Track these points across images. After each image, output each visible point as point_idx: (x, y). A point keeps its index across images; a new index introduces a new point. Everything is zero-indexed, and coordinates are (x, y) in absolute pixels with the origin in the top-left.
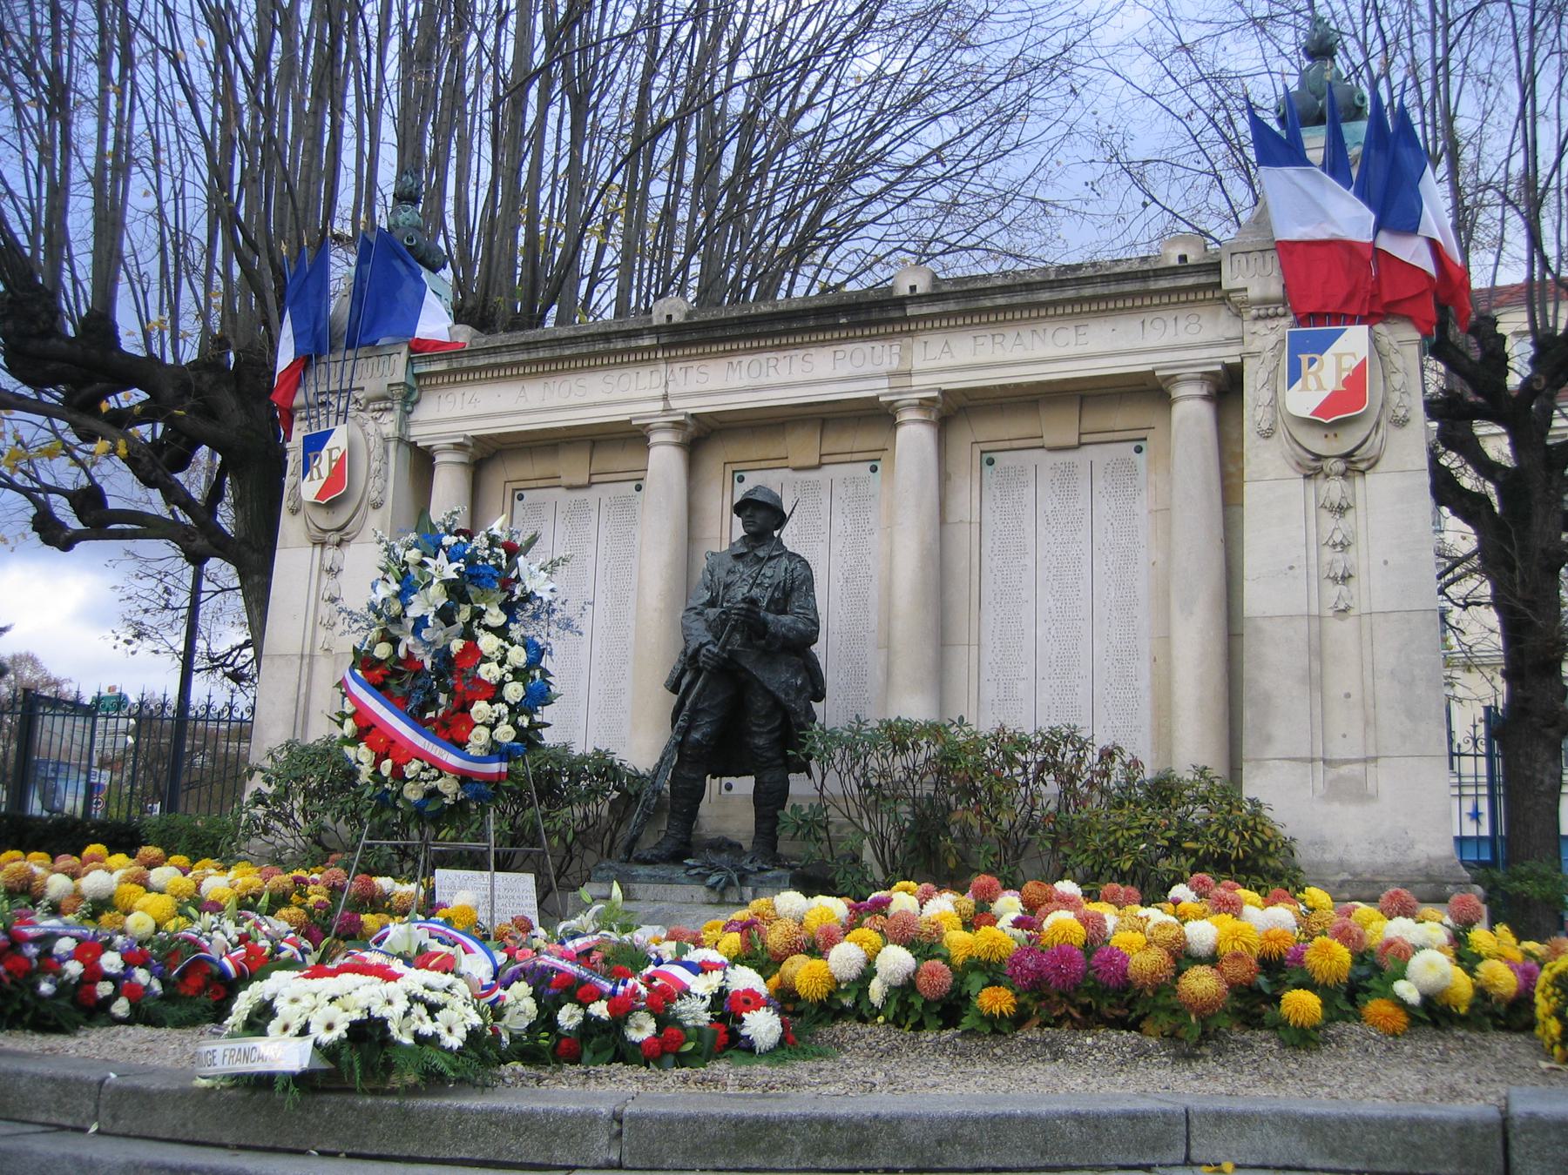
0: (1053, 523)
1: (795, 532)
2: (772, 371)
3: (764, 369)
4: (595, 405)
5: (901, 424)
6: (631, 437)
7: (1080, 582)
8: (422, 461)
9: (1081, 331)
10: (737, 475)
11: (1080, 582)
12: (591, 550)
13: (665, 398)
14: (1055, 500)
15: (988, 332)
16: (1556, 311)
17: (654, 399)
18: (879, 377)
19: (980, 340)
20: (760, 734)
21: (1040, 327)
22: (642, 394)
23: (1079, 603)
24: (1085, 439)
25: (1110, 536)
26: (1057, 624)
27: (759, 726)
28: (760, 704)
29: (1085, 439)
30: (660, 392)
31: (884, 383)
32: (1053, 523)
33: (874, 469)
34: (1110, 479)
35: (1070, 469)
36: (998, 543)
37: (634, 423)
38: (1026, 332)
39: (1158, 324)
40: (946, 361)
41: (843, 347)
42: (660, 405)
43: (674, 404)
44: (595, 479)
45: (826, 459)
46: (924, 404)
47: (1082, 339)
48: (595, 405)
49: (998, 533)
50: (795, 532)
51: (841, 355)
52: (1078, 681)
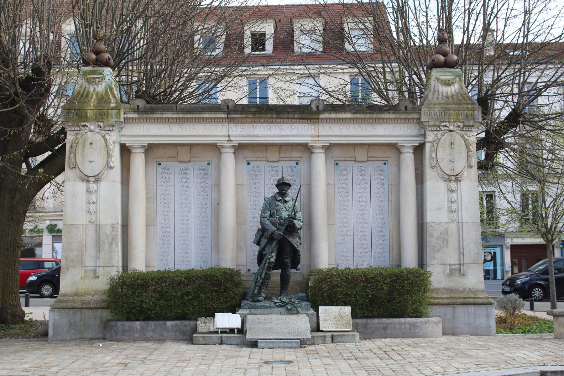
0: (358, 186)
1: (270, 183)
2: (269, 130)
3: (266, 129)
4: (201, 136)
5: (314, 153)
6: (215, 148)
7: (367, 205)
8: (125, 150)
9: (374, 127)
10: (247, 162)
11: (367, 205)
12: (191, 185)
13: (229, 136)
14: (359, 179)
15: (344, 125)
16: (510, 137)
17: (225, 137)
18: (308, 136)
19: (342, 127)
20: (287, 258)
21: (361, 126)
22: (220, 134)
23: (366, 212)
24: (369, 159)
25: (376, 191)
26: (360, 218)
27: (287, 256)
28: (288, 249)
29: (369, 159)
30: (226, 133)
31: (310, 139)
32: (358, 186)
33: (297, 164)
34: (375, 172)
35: (364, 167)
36: (340, 191)
37: (218, 144)
38: (357, 126)
39: (399, 128)
40: (330, 133)
41: (295, 124)
42: (227, 139)
43: (232, 139)
44: (192, 159)
45: (281, 159)
46: (323, 147)
47: (375, 130)
48: (201, 136)
49: (340, 188)
50: (270, 183)
51: (293, 127)
52: (367, 237)
